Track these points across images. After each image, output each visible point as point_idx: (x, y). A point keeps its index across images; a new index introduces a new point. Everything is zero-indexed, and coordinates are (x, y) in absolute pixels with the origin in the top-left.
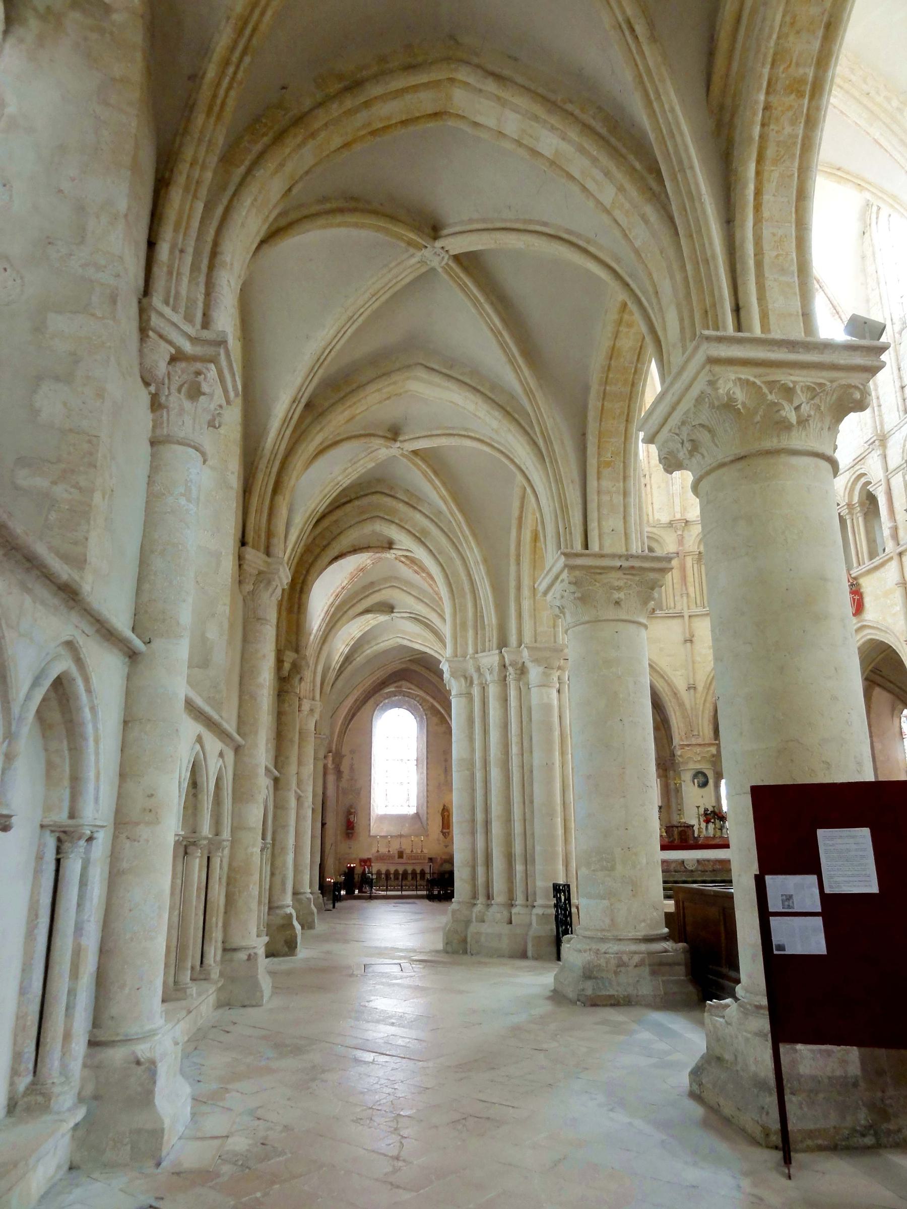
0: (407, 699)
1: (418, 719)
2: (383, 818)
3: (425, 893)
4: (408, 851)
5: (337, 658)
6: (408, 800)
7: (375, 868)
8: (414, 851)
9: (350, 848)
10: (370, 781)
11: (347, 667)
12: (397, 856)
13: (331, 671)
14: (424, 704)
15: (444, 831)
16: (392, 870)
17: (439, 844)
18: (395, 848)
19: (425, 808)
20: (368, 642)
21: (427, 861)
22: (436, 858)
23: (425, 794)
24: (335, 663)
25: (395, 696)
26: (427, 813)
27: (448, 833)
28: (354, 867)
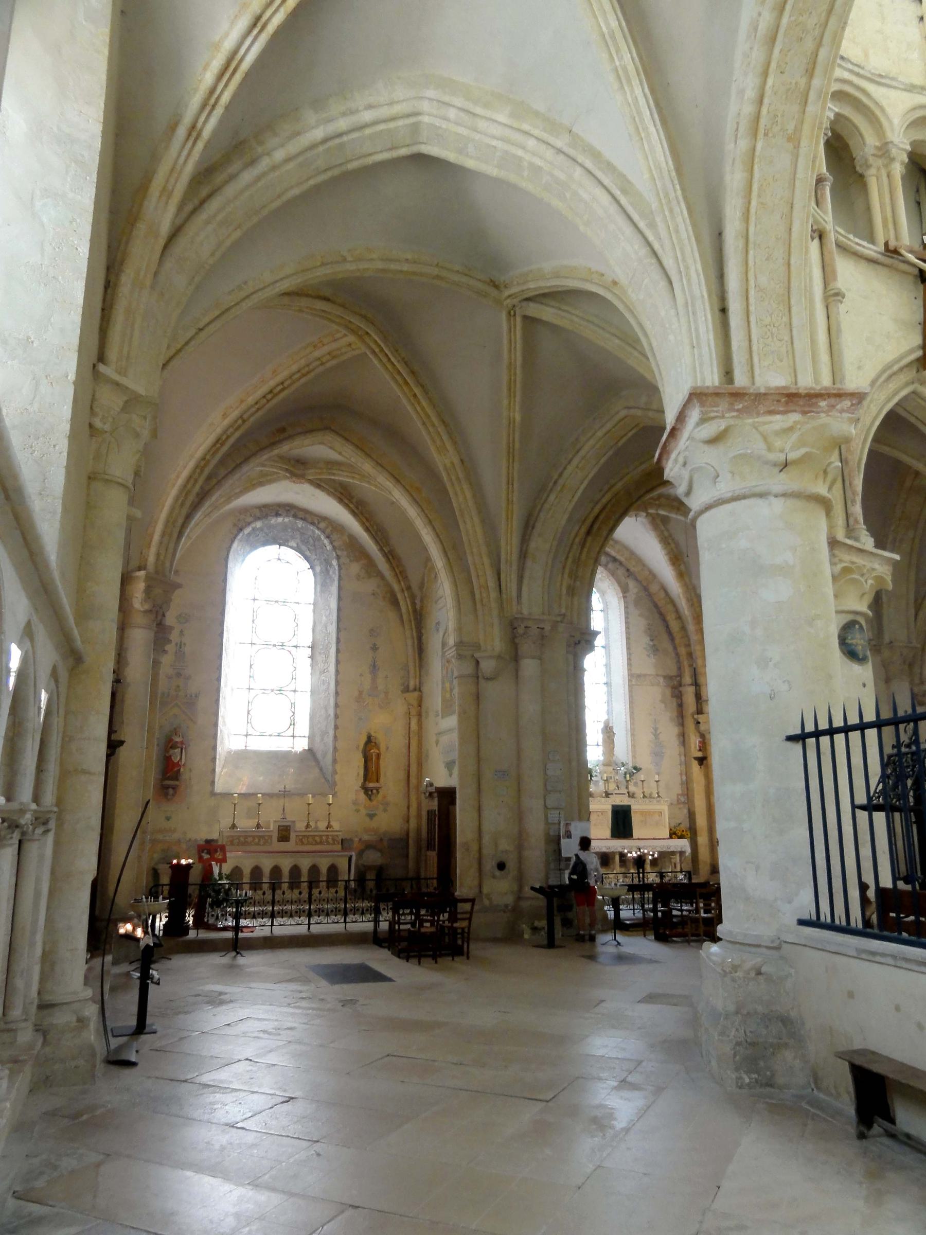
0: (300, 524)
1: (318, 569)
2: (242, 756)
3: (363, 925)
4: (300, 826)
5: (209, 78)
6: (293, 724)
7: (235, 859)
8: (312, 824)
9: (168, 819)
10: (219, 679)
11: (232, 177)
12: (275, 838)
13: (181, 132)
14: (335, 536)
15: (371, 785)
16: (267, 865)
17: (358, 811)
18: (271, 817)
19: (329, 739)
20: (318, 104)
21: (339, 847)
22: (351, 840)
23: (331, 712)
24: (195, 101)
25: (277, 515)
26: (335, 749)
27: (377, 789)
28: (189, 866)
